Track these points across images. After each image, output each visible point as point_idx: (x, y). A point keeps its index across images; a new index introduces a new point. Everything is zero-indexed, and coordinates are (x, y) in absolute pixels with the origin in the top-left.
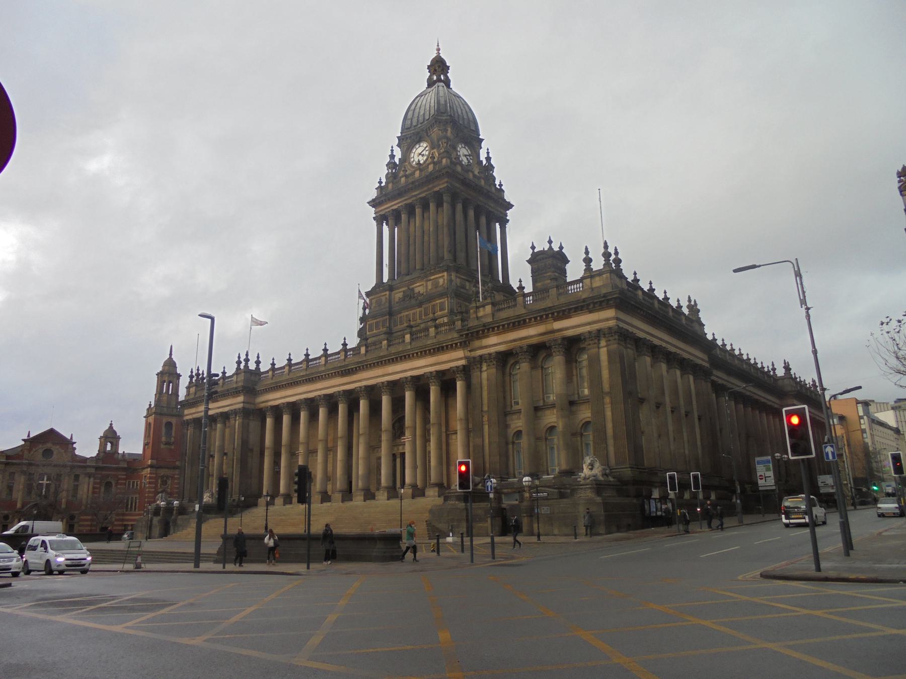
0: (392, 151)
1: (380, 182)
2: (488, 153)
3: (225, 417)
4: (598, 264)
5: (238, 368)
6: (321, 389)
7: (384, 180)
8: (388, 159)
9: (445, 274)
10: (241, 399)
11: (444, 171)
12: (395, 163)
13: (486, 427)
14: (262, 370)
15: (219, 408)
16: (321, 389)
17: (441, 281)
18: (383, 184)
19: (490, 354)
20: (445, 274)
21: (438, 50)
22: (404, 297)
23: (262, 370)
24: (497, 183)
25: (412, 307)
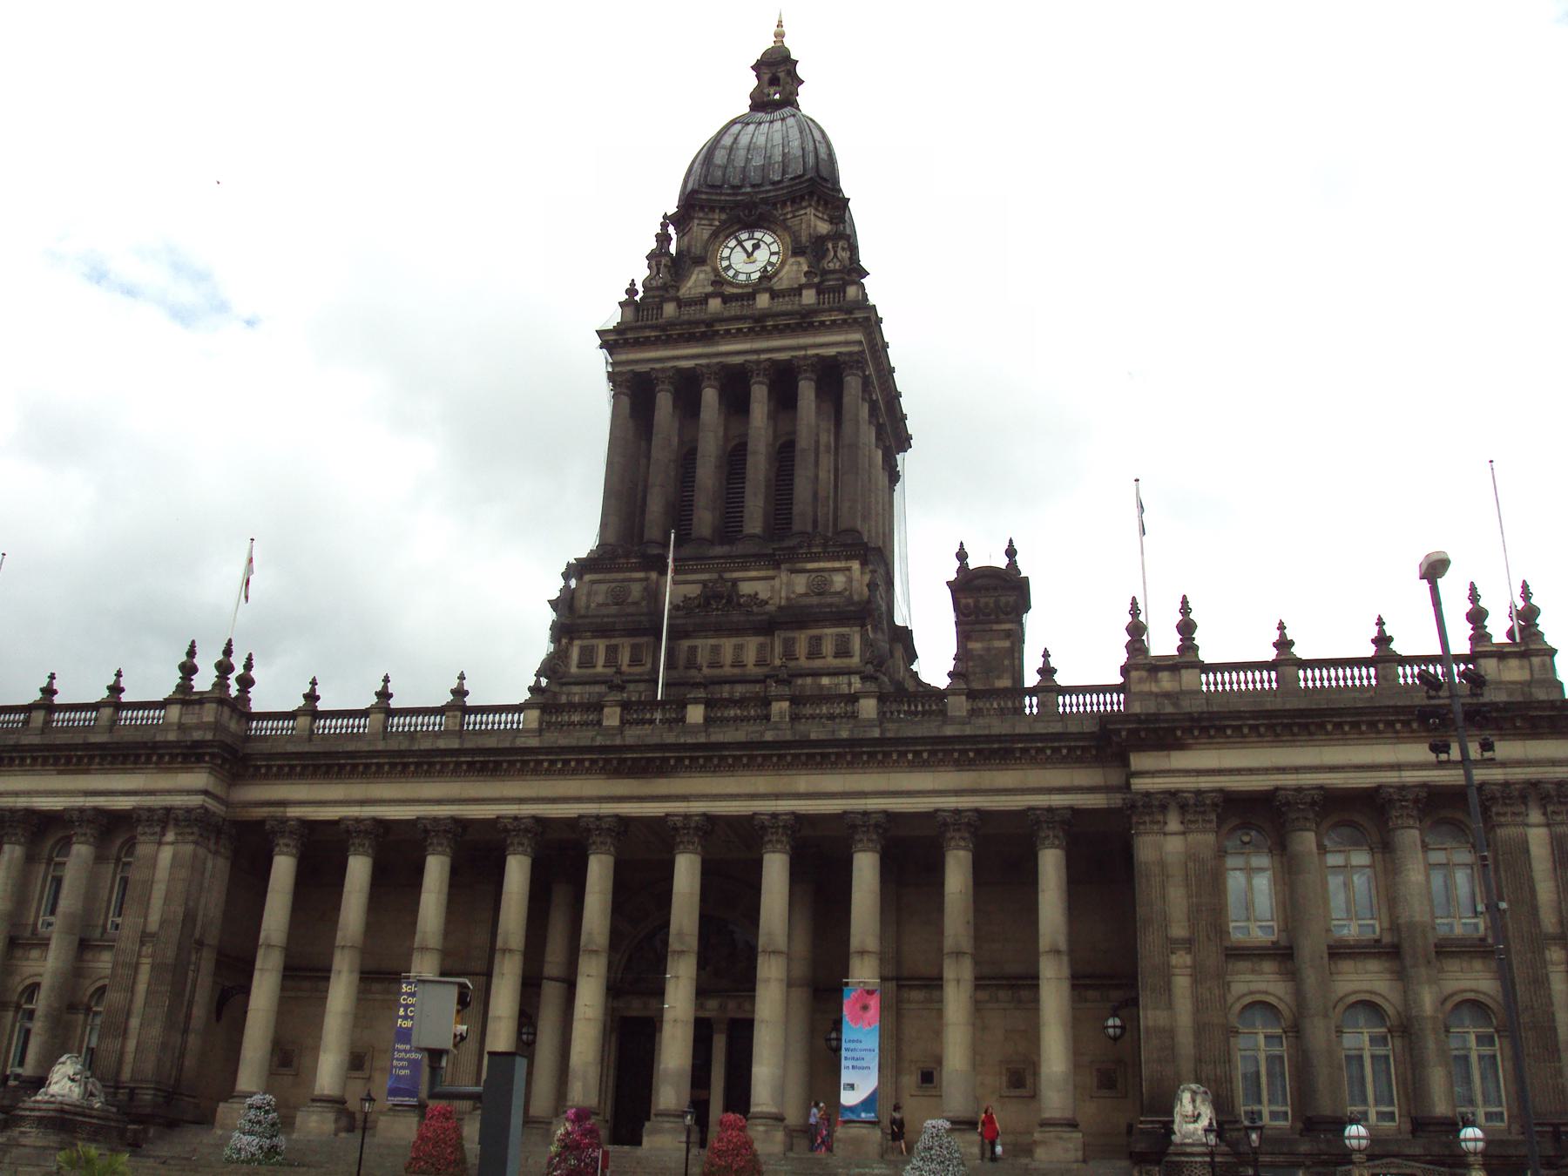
3: (114, 830)
4: (1499, 628)
5: (185, 686)
6: (522, 801)
9: (856, 565)
10: (198, 779)
12: (668, 253)
13: (1182, 983)
14: (256, 706)
15: (87, 793)
16: (522, 801)
17: (839, 581)
18: (637, 298)
19: (1199, 793)
20: (856, 565)
22: (710, 597)
23: (256, 706)
25: (736, 631)
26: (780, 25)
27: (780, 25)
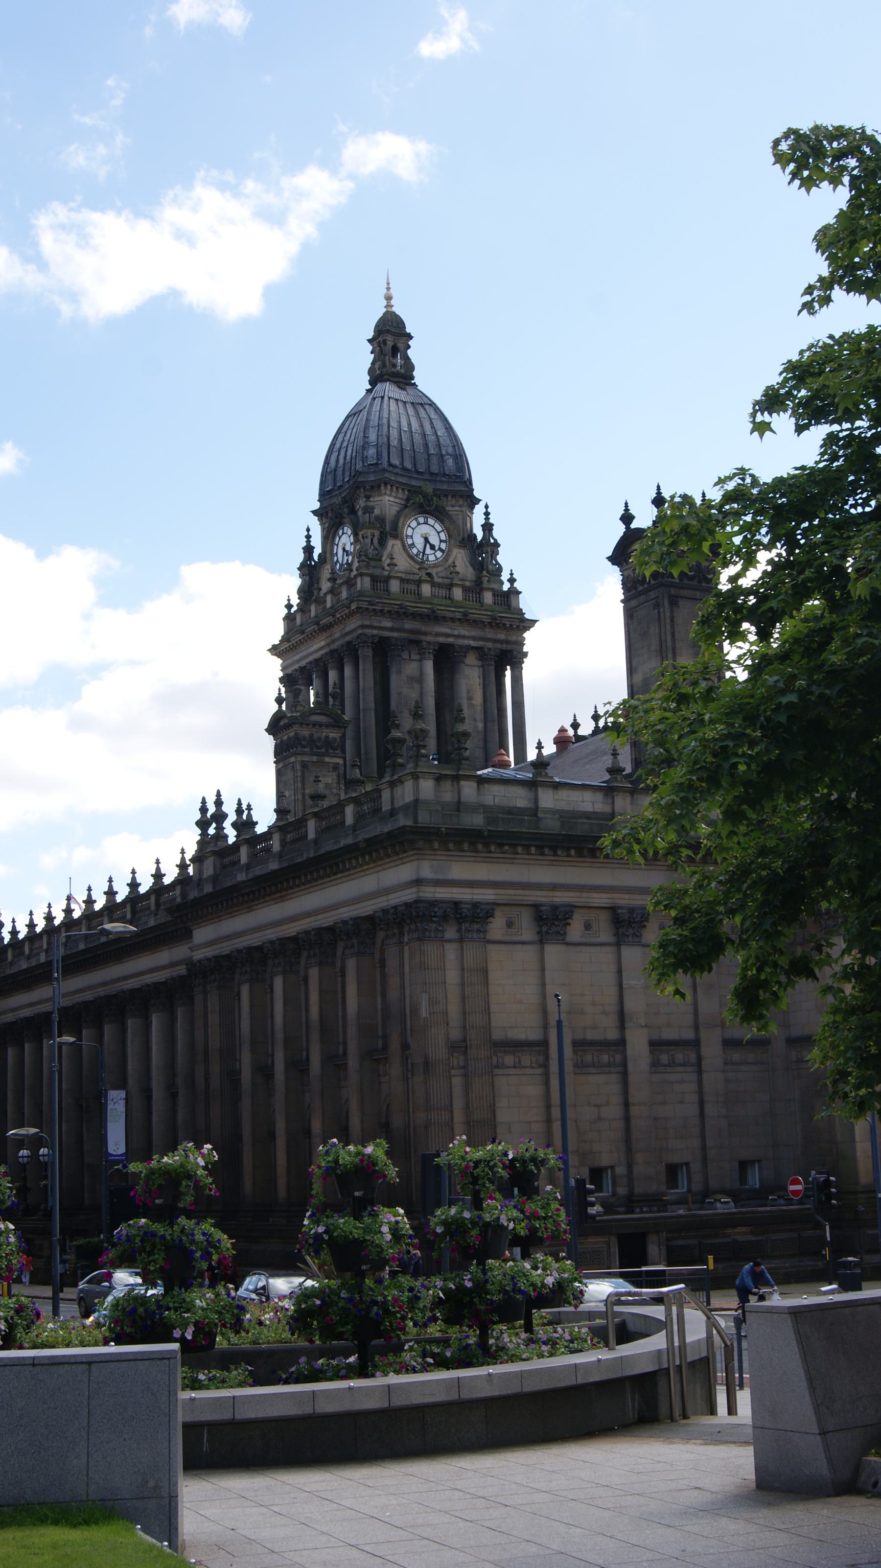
0: (308, 537)
1: (289, 606)
2: (487, 514)
7: (295, 601)
8: (300, 557)
11: (354, 606)
18: (292, 611)
21: (389, 298)
24: (505, 576)
26: (388, 289)
27: (388, 289)
